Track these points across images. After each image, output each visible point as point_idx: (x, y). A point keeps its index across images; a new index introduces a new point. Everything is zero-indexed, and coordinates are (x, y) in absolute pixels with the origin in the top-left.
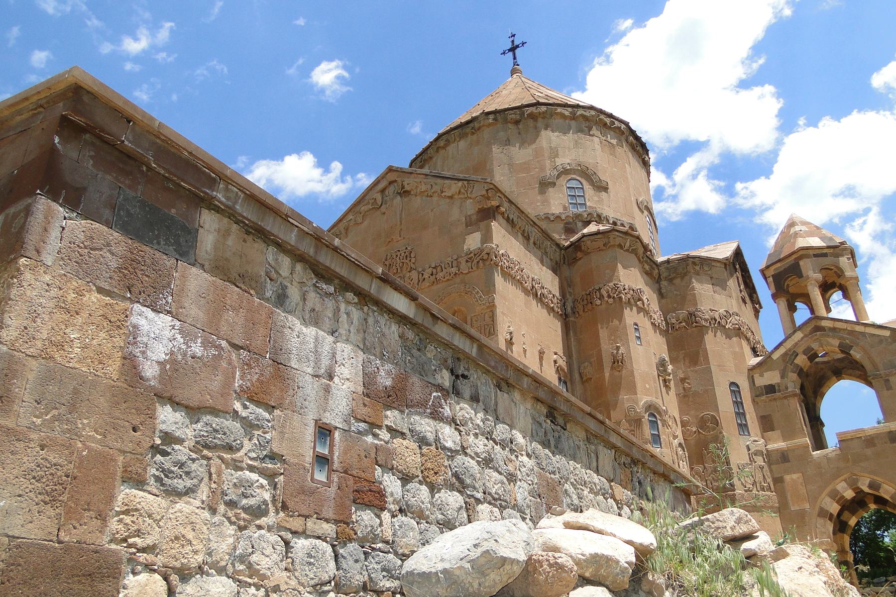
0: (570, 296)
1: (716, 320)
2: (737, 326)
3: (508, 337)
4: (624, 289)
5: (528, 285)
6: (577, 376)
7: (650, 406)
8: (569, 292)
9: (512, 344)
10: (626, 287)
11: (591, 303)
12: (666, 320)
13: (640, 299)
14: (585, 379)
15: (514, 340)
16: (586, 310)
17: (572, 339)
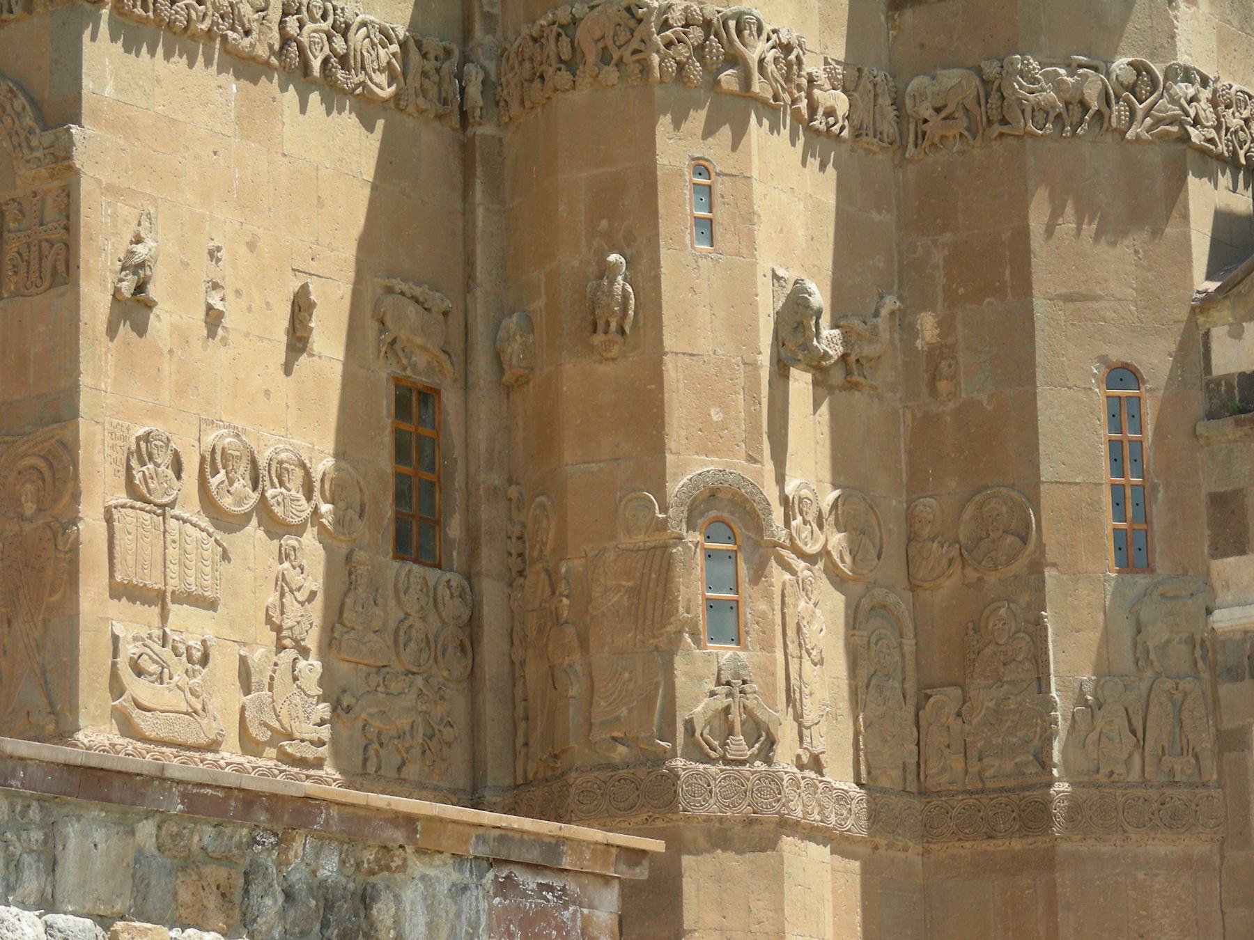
0: (490, 28)
1: (1085, 107)
2: (1175, 129)
3: (127, 287)
4: (666, 25)
5: (262, 43)
6: (482, 363)
7: (713, 494)
8: (488, 16)
9: (149, 305)
10: (676, 16)
11: (542, 77)
12: (897, 103)
13: (734, 60)
14: (508, 377)
15: (153, 291)
16: (528, 104)
17: (480, 212)
